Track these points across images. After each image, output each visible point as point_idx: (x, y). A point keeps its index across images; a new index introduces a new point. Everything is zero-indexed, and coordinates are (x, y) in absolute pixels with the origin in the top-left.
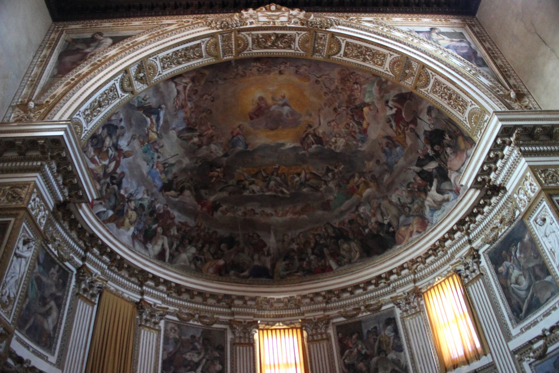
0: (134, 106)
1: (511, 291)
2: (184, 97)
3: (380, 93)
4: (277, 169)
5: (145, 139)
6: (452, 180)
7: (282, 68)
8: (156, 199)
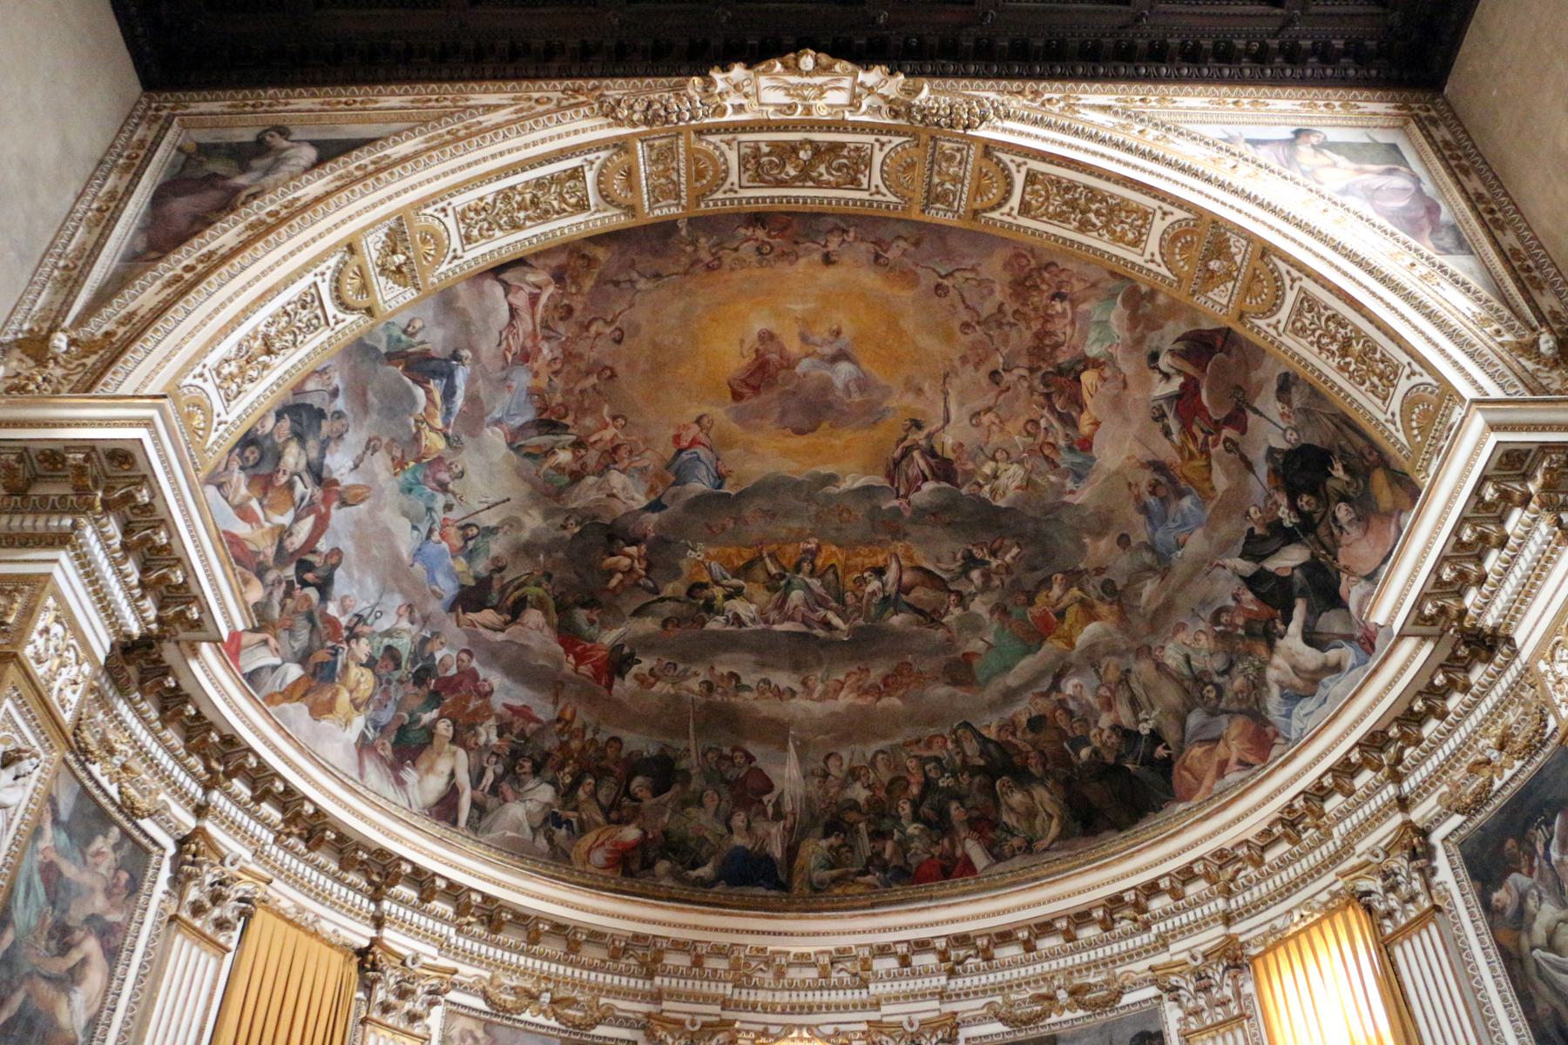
0: (375, 349)
1: (1532, 969)
2: (530, 328)
3: (1132, 328)
4: (814, 553)
5: (406, 454)
6: (1353, 606)
7: (832, 246)
8: (436, 635)
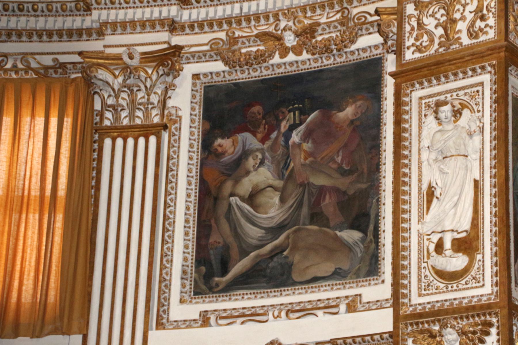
1: (222, 209)
